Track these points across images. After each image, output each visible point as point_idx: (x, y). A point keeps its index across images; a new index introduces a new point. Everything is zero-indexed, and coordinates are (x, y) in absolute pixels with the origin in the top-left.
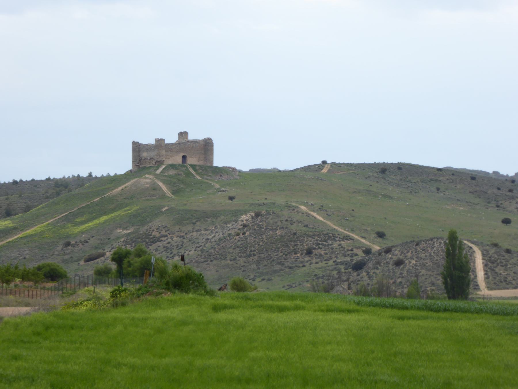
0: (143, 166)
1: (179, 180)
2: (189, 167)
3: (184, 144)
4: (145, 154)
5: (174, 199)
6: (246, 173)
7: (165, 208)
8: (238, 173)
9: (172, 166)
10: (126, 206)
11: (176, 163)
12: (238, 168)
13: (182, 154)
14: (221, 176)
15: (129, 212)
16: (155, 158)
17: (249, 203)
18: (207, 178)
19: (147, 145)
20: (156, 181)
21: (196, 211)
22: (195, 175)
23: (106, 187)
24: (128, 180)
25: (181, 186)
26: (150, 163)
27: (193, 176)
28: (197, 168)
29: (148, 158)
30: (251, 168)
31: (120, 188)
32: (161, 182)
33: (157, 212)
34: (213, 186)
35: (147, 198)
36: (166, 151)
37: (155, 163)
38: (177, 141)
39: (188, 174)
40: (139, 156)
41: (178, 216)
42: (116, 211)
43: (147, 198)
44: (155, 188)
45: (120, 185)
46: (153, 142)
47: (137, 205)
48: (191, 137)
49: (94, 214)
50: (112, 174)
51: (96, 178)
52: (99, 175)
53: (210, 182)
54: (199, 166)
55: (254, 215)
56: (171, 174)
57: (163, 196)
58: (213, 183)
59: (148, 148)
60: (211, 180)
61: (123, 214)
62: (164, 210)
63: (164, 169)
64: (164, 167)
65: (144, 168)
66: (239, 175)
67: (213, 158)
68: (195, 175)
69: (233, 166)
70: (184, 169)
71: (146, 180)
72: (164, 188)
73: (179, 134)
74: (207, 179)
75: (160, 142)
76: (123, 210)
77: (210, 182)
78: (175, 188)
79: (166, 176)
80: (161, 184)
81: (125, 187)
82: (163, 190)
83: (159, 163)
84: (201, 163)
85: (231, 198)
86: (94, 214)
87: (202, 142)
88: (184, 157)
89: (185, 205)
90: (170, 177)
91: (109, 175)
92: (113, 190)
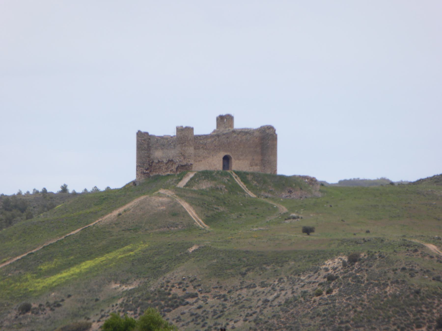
0: (154, 174)
1: (218, 198)
2: (234, 175)
3: (227, 136)
4: (158, 154)
5: (209, 232)
6: (333, 187)
7: (194, 248)
8: (318, 187)
9: (206, 175)
10: (126, 244)
11: (212, 169)
12: (320, 178)
13: (222, 154)
14: (290, 192)
15: (132, 253)
16: (177, 160)
17: (338, 240)
18: (266, 194)
19: (162, 138)
20: (178, 199)
21: (247, 252)
22: (246, 190)
23: (92, 210)
24: (131, 198)
25: (222, 209)
26: (167, 169)
27: (242, 191)
28: (249, 178)
29: (165, 161)
30: (343, 179)
31: (116, 213)
32: (186, 201)
33: (179, 255)
34: (276, 209)
35: (162, 230)
36: (195, 149)
37: (177, 169)
38: (214, 131)
39: (234, 189)
40: (149, 157)
41: (215, 261)
42: (108, 253)
43: (162, 230)
44: (176, 213)
45: (116, 208)
46: (172, 132)
47: (144, 242)
48: (238, 125)
49: (72, 257)
50: (102, 188)
51: (75, 194)
52: (79, 190)
53: (271, 202)
54: (253, 174)
55: (346, 260)
56: (204, 187)
57: (190, 227)
58: (276, 205)
59: (163, 142)
60: (273, 199)
61: (120, 256)
62: (191, 250)
63: (191, 179)
64: (191, 175)
65: (157, 178)
66: (321, 191)
67: (275, 161)
68: (246, 190)
69: (312, 175)
70: (225, 179)
71: (161, 199)
72: (192, 212)
73: (217, 119)
74: (267, 197)
75: (184, 133)
76: (121, 250)
77: (271, 202)
78: (210, 213)
79: (194, 191)
80: (186, 205)
81: (125, 211)
82: (189, 216)
83: (184, 169)
84: (256, 169)
85: (308, 231)
86: (72, 257)
87: (257, 134)
88: (227, 159)
89: (228, 242)
90: (202, 193)
91: (96, 190)
92: (103, 215)
